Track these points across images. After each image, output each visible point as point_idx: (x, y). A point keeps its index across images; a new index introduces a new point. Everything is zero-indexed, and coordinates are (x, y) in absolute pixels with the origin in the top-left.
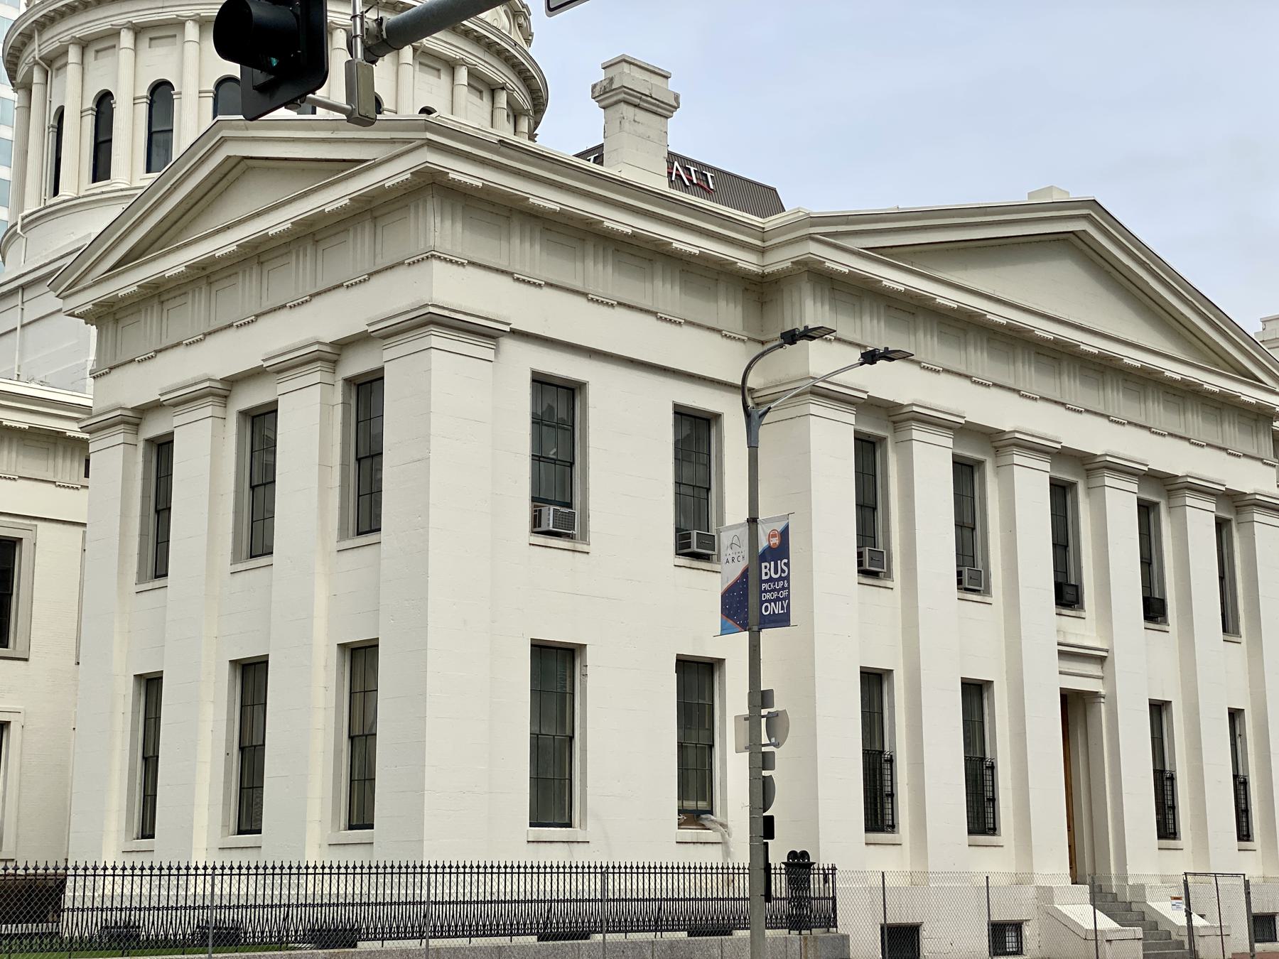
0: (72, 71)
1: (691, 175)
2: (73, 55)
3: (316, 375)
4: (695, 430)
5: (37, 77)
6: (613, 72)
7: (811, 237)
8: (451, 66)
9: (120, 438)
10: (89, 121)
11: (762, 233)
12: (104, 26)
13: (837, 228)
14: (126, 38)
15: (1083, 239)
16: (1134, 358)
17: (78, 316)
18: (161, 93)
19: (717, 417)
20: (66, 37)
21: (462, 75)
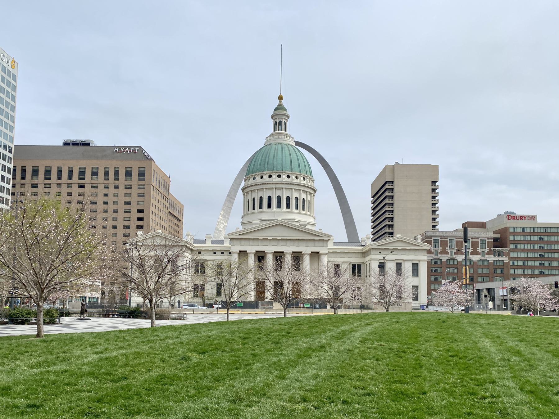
8: (307, 192)
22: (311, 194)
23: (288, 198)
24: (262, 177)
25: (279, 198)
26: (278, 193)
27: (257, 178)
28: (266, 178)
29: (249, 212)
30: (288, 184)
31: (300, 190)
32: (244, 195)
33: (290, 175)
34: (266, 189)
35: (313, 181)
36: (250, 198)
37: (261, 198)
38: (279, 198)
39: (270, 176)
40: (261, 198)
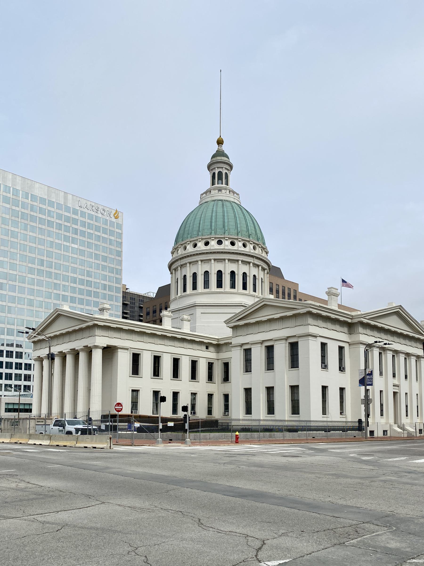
0: (188, 268)
1: (340, 306)
2: (188, 265)
3: (284, 342)
4: (341, 349)
5: (179, 268)
6: (330, 290)
7: (362, 317)
8: (258, 266)
9: (239, 348)
10: (192, 278)
11: (352, 316)
12: (196, 260)
13: (364, 316)
14: (200, 262)
15: (399, 313)
16: (405, 333)
17: (230, 328)
18: (206, 273)
19: (344, 347)
20: (187, 262)
21: (260, 268)
22: (264, 269)
23: (233, 274)
24: (195, 246)
25: (220, 274)
26: (219, 266)
27: (188, 247)
28: (201, 246)
29: (179, 294)
30: (233, 253)
31: (249, 263)
32: (171, 273)
33: (236, 241)
34: (202, 261)
35: (267, 253)
36: (179, 275)
37: (195, 276)
38: (220, 274)
39: (207, 244)
40: (195, 276)
